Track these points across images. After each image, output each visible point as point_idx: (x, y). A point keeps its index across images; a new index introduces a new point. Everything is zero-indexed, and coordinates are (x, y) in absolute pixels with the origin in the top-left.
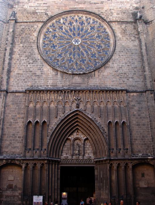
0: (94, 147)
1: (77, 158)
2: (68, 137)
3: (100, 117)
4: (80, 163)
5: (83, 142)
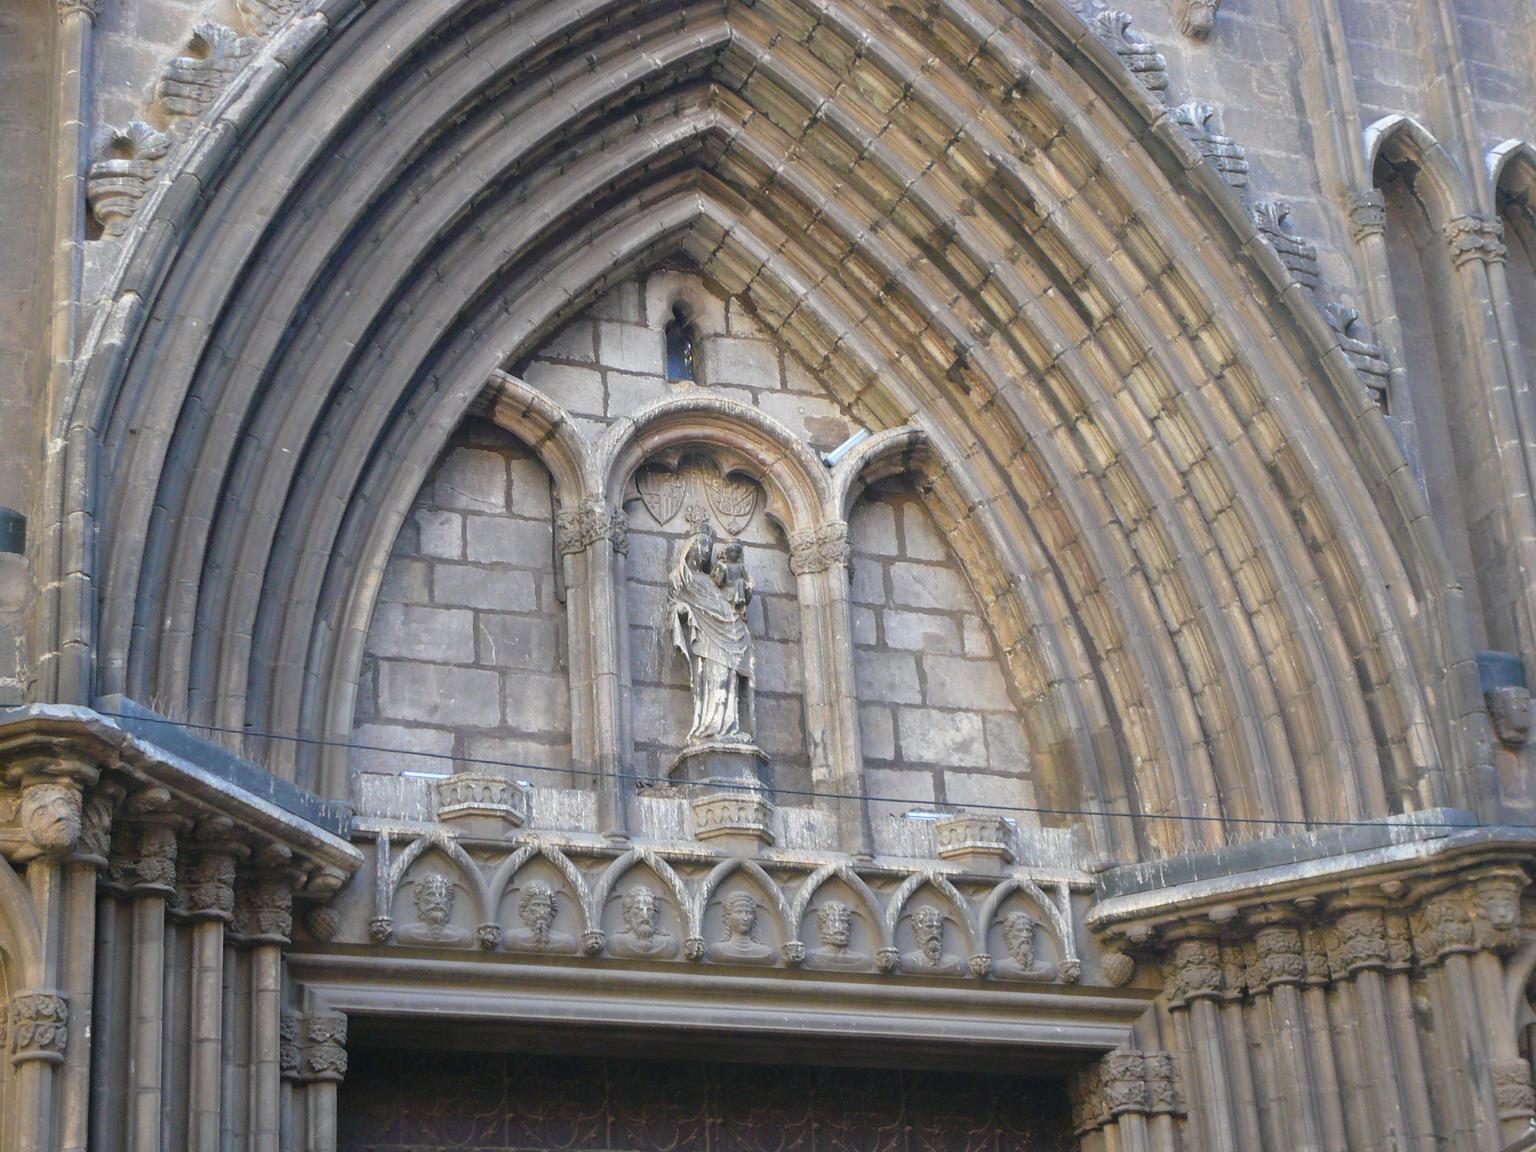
0: (1077, 644)
1: (746, 852)
2: (520, 387)
3: (1200, 35)
4: (795, 968)
5: (835, 509)
